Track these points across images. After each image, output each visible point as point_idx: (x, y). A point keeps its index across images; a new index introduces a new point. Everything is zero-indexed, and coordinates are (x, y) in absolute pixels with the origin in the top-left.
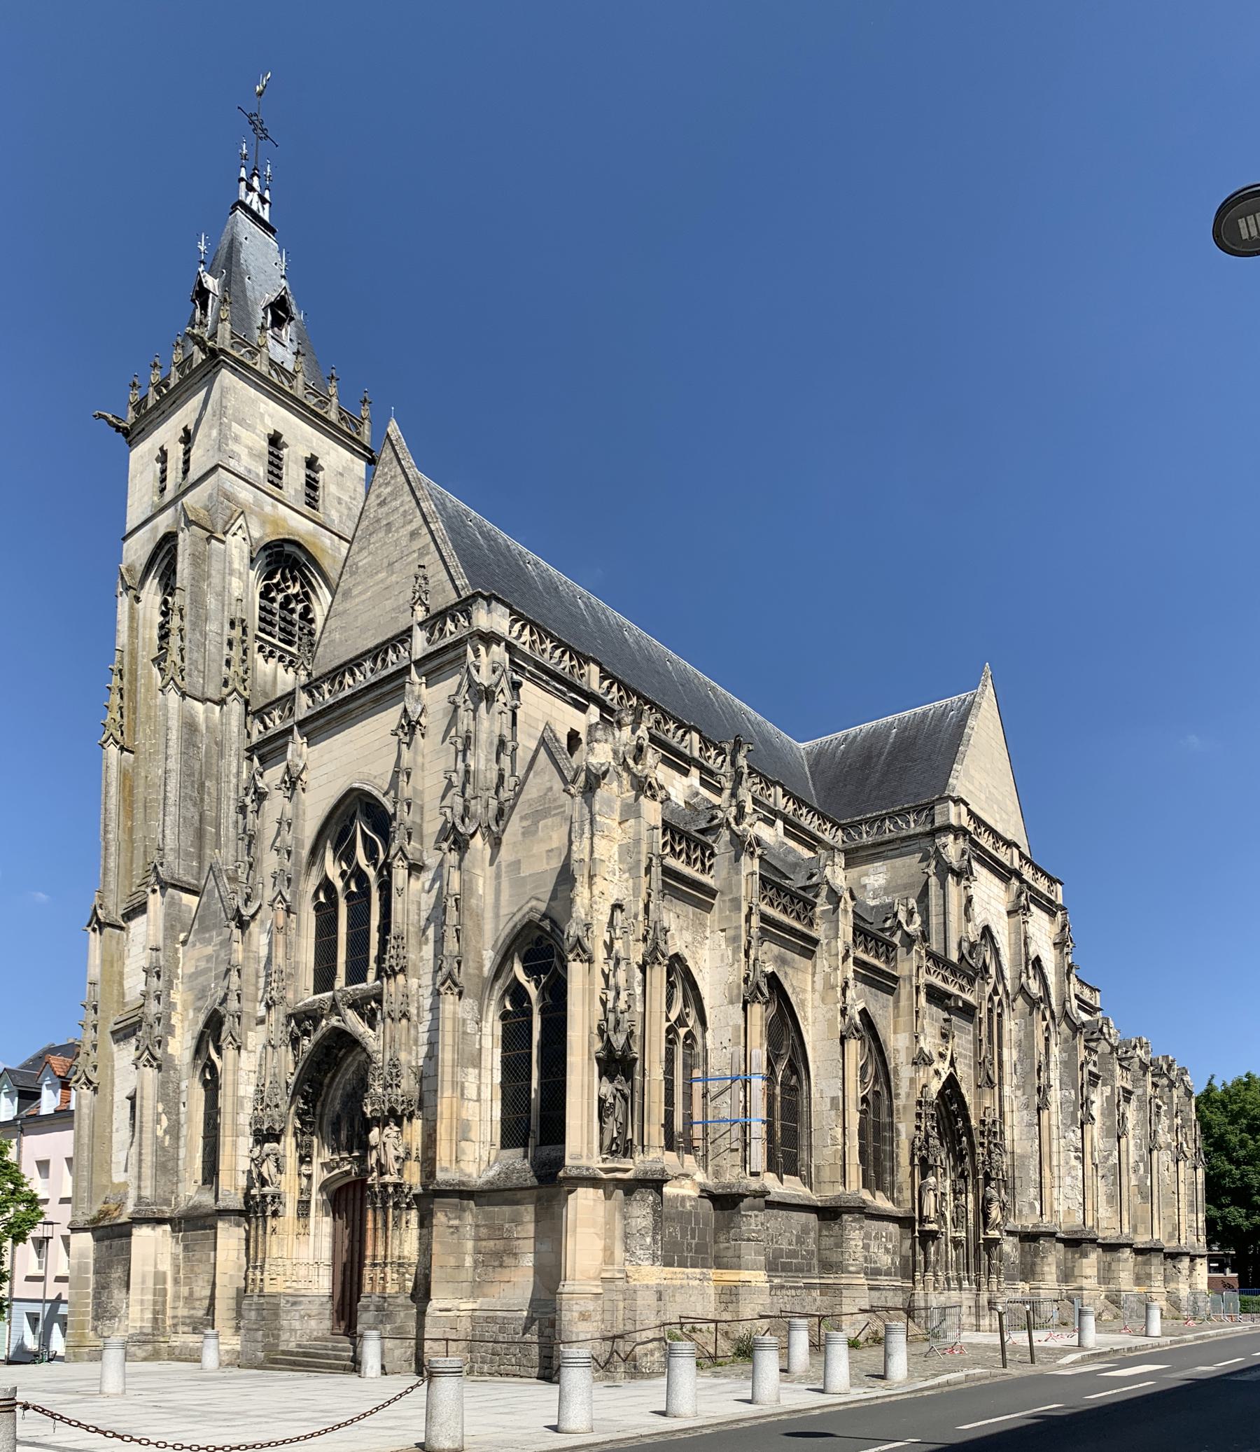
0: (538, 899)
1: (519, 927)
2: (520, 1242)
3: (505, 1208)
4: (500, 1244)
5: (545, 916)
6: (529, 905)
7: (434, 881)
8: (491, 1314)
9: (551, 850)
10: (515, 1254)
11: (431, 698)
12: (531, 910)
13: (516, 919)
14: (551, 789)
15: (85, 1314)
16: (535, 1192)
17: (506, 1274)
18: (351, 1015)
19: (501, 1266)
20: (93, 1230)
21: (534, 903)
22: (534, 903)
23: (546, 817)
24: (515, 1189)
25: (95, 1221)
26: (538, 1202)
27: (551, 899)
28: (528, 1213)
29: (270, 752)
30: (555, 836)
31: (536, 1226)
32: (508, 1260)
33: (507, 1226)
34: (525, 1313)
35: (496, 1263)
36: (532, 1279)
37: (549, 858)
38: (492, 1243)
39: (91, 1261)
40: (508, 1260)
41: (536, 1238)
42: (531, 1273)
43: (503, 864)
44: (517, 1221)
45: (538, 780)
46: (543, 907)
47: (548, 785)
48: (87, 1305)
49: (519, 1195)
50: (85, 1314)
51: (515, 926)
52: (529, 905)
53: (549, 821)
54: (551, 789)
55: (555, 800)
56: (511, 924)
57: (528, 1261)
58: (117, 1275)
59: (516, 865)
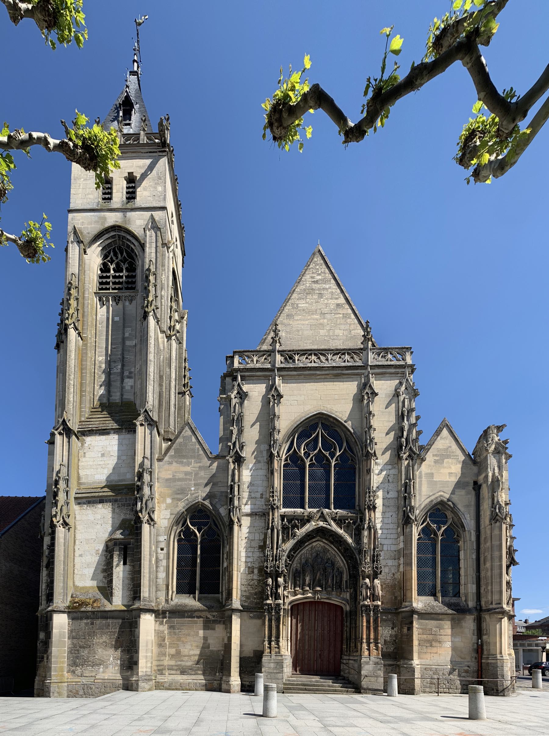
0: (443, 492)
1: (435, 502)
2: (441, 637)
3: (432, 622)
4: (430, 637)
5: (449, 500)
6: (439, 494)
7: (382, 471)
8: (429, 667)
9: (452, 473)
10: (440, 641)
11: (384, 387)
12: (441, 496)
13: (433, 498)
14: (450, 447)
15: (63, 662)
16: (451, 616)
17: (434, 650)
18: (332, 523)
19: (431, 646)
20: (69, 613)
21: (442, 493)
22: (442, 493)
23: (447, 458)
24: (439, 614)
25: (68, 607)
26: (452, 620)
27: (451, 494)
28: (447, 625)
29: (249, 376)
30: (453, 467)
31: (452, 630)
32: (434, 644)
33: (434, 629)
34: (449, 667)
35: (428, 645)
36: (450, 653)
37: (450, 476)
38: (425, 636)
39: (67, 631)
40: (434, 644)
41: (452, 635)
42: (450, 649)
43: (423, 473)
44: (440, 628)
45: (442, 441)
46: (447, 496)
47: (449, 445)
48: (64, 657)
49: (441, 617)
50: (63, 662)
51: (432, 501)
52: (439, 494)
53: (450, 460)
54: (450, 447)
55: (453, 452)
56: (429, 500)
57: (448, 644)
58: (101, 641)
59: (431, 475)
